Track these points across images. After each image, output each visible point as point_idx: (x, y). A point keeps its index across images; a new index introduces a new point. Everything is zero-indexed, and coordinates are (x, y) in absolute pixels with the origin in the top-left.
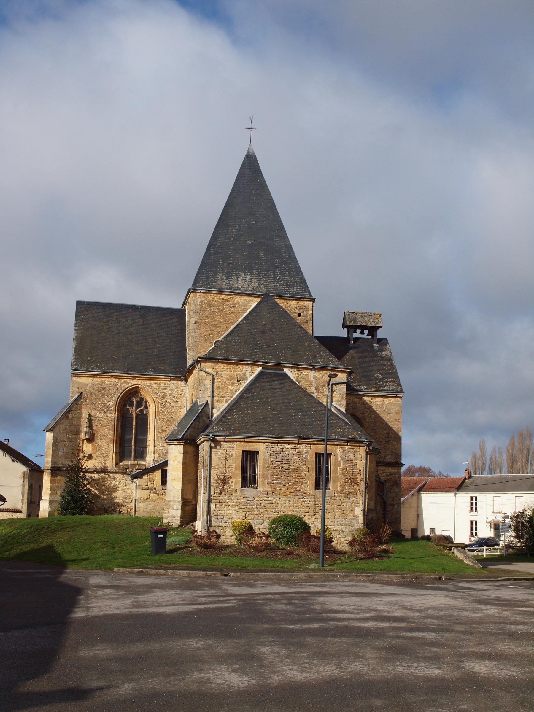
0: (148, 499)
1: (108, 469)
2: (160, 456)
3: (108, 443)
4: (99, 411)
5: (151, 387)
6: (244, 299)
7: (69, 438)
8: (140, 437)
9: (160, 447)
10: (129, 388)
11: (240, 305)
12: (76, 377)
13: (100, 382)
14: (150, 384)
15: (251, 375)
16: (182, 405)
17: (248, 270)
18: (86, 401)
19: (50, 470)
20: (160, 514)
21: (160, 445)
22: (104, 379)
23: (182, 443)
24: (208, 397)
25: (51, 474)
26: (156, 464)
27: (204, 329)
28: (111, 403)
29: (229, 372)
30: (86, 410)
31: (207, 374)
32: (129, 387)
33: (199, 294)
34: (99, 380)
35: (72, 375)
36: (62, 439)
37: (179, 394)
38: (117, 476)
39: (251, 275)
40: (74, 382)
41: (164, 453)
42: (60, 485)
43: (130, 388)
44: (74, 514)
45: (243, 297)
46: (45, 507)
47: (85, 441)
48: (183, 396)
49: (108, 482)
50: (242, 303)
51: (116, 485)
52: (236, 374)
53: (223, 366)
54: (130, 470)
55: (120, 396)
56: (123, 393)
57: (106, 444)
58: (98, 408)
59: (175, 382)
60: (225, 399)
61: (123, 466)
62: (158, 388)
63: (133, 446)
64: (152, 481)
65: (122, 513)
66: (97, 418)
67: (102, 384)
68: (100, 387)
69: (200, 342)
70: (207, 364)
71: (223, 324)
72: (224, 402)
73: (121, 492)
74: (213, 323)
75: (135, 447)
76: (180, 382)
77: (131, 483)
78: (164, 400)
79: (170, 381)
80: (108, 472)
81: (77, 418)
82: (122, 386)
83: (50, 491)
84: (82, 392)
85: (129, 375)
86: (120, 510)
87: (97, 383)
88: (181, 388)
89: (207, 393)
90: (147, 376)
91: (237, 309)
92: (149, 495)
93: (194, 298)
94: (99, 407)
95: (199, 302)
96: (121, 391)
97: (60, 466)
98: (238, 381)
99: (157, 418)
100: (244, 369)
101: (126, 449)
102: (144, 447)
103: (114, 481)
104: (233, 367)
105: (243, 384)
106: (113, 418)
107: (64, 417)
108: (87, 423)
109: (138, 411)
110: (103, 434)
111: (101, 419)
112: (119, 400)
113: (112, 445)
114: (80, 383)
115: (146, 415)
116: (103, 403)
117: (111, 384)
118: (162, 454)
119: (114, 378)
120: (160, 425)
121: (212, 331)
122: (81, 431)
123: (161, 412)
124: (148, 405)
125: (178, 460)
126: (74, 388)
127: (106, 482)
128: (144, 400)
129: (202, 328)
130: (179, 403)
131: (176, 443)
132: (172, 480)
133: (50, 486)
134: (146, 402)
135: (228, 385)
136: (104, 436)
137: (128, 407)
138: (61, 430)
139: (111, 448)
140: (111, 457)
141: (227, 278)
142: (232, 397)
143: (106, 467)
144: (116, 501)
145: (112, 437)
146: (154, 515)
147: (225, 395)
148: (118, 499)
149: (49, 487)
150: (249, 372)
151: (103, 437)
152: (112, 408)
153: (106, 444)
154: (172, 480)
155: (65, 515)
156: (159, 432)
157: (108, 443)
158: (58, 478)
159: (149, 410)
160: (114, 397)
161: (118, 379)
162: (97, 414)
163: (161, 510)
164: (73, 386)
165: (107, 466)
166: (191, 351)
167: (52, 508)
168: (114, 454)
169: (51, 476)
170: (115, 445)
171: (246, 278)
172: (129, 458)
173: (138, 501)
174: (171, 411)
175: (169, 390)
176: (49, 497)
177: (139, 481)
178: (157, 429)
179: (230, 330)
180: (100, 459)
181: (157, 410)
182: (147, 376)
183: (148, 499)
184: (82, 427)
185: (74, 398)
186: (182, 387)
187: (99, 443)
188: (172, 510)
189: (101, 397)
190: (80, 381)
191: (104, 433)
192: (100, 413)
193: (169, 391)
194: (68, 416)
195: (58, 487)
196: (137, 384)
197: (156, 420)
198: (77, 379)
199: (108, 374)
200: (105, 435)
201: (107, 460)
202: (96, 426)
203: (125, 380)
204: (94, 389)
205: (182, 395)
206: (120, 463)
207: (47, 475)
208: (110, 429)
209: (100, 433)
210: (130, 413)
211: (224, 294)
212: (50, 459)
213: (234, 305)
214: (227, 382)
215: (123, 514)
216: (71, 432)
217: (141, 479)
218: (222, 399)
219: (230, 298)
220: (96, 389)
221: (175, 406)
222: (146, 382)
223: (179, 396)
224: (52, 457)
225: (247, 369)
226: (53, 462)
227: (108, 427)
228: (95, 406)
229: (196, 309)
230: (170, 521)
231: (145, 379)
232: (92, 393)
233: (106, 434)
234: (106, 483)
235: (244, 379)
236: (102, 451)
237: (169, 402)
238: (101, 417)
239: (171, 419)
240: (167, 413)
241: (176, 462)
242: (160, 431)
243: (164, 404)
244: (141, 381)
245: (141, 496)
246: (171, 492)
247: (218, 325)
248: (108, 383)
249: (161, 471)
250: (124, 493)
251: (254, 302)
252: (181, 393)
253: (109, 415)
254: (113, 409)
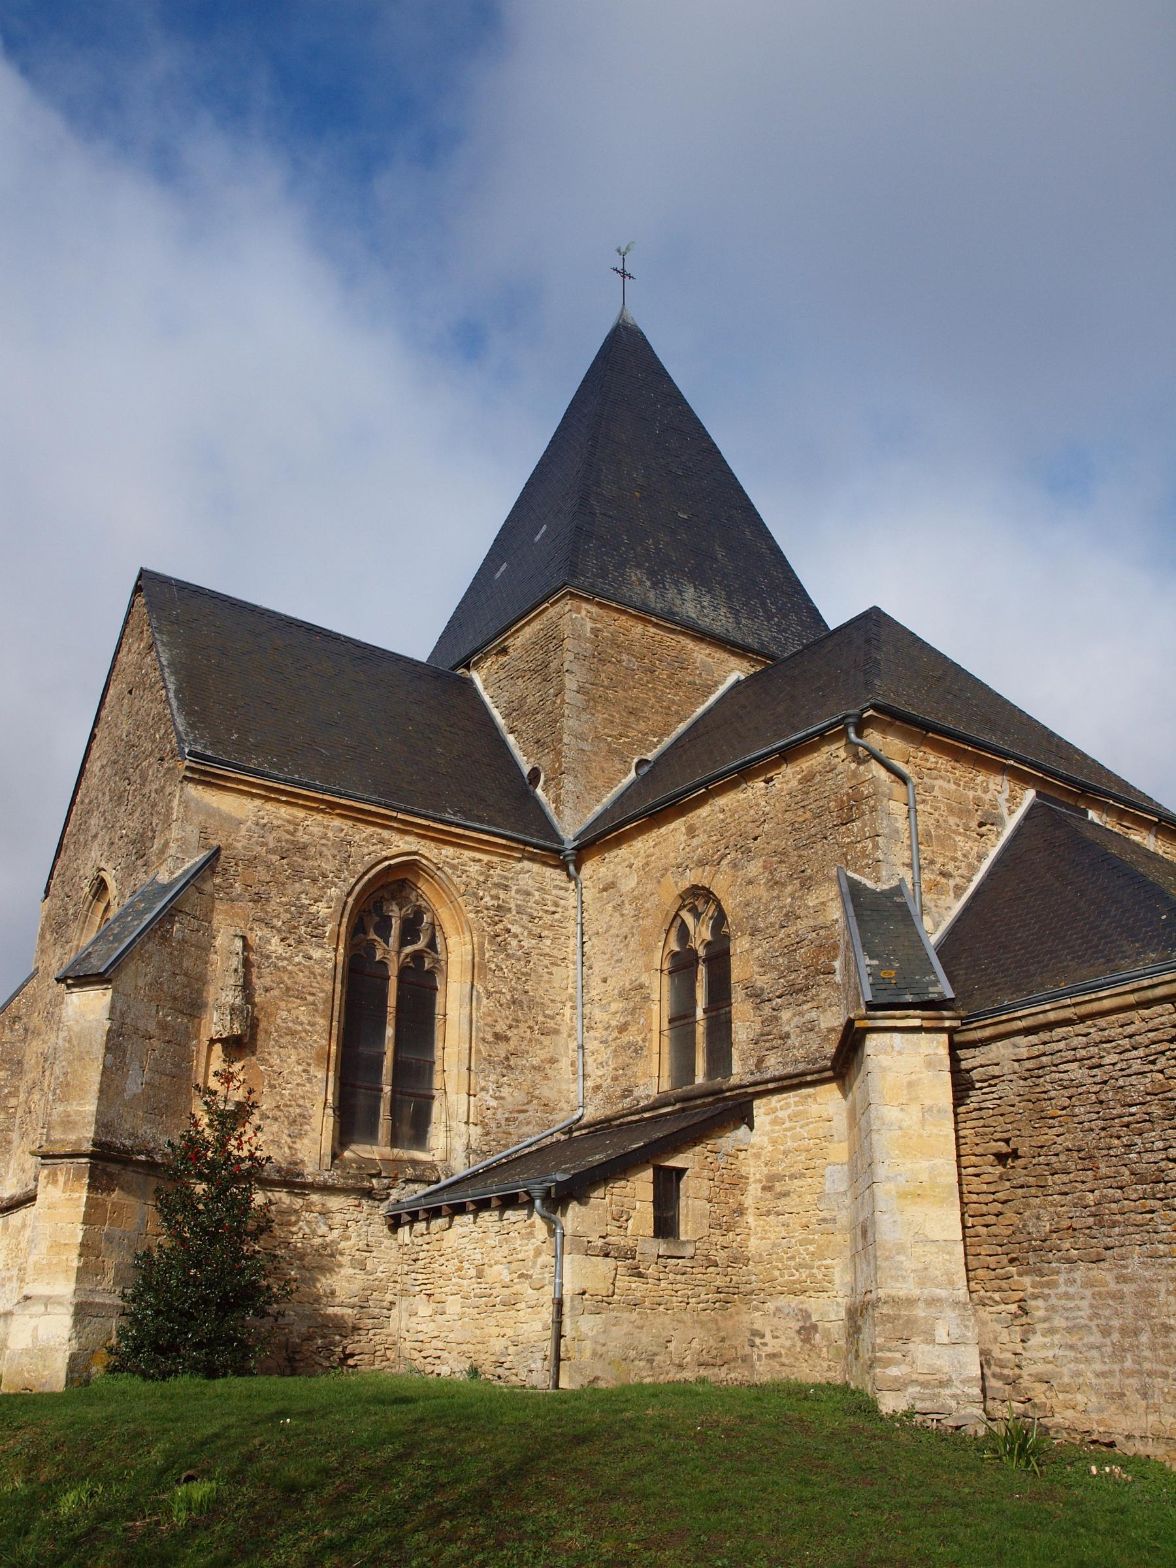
0: (603, 1303)
1: (306, 1172)
2: (488, 1134)
3: (309, 1065)
4: (279, 931)
5: (459, 873)
6: (707, 651)
7: (163, 1026)
8: (409, 1056)
9: (488, 1098)
10: (387, 863)
11: (697, 668)
12: (200, 788)
13: (288, 821)
14: (456, 861)
15: (1011, 812)
16: (555, 953)
17: (702, 579)
18: (232, 886)
19: (90, 1155)
20: (652, 1368)
21: (488, 1092)
22: (301, 814)
23: (947, 1024)
24: (904, 864)
25: (90, 1177)
26: (479, 1165)
27: (605, 716)
28: (322, 909)
29: (953, 787)
30: (229, 921)
31: (893, 777)
32: (386, 859)
33: (589, 607)
34: (285, 812)
35: (189, 774)
36: (141, 1025)
37: (546, 912)
38: (335, 1202)
39: (709, 596)
40: (192, 805)
41: (503, 1123)
42: (118, 1232)
43: (392, 862)
44: (212, 1373)
45: (703, 646)
46: (41, 1333)
47: (218, 1047)
48: (559, 921)
49: (300, 1228)
50: (703, 663)
51: (332, 1241)
52: (974, 798)
53: (934, 760)
54: (386, 1181)
55: (358, 888)
56: (366, 878)
57: (301, 1068)
58: (275, 921)
59: (535, 867)
60: (952, 883)
61: (363, 1163)
62: (482, 879)
63: (387, 1089)
64: (622, 1218)
65: (351, 1362)
66: (268, 957)
67: (296, 830)
68: (287, 841)
69: (595, 754)
70: (889, 738)
71: (657, 712)
72: (952, 894)
73: (351, 1271)
74: (629, 703)
75: (393, 1091)
76: (549, 872)
77: (385, 1237)
78: (500, 926)
79: (520, 860)
80: (304, 1186)
81: (198, 947)
82: (366, 851)
83: (80, 1255)
84: (219, 850)
85: (395, 814)
86: (343, 1351)
87: (276, 823)
88: (554, 892)
89: (898, 849)
90: (453, 829)
91: (691, 678)
92: (613, 1284)
93: (574, 616)
94: (278, 916)
95: (589, 629)
96: (360, 869)
97: (128, 1143)
98: (981, 825)
99: (479, 987)
100: (992, 786)
101: (361, 1100)
102: (420, 1096)
103: (325, 1224)
104: (962, 771)
105: (992, 837)
106: (330, 965)
107: (154, 931)
108: (236, 970)
109: (407, 956)
110: (290, 1025)
111: (285, 963)
112: (351, 900)
113: (321, 1074)
114: (211, 812)
115: (431, 974)
116: (295, 905)
117: (325, 836)
118: (494, 1125)
119: (338, 815)
120: (489, 1015)
121: (626, 725)
122: (205, 1005)
123: (493, 966)
124: (438, 940)
125: (928, 1102)
126: (189, 828)
127: (294, 1229)
128: (426, 918)
129: (598, 711)
130: (548, 942)
131: (917, 1023)
132: (903, 1195)
133: (81, 1233)
134: (433, 925)
135: (955, 832)
136: (293, 1033)
137: (373, 936)
138: (141, 983)
139: (318, 1088)
140: (316, 1121)
141: (654, 585)
142: (970, 880)
143: (296, 1164)
144: (330, 1311)
145: (324, 1042)
146: (632, 1374)
147: (950, 867)
148: (338, 1300)
149: (76, 1235)
150: (1007, 800)
151: (289, 1038)
152: (328, 929)
153: (301, 1068)
154: (903, 1195)
155: (165, 1375)
156: (484, 1039)
157: (309, 1065)
158: (115, 1195)
159: (442, 957)
160: (335, 885)
161: (350, 823)
162: (269, 942)
163: (659, 1350)
164: (185, 819)
165: (302, 1161)
166: (571, 778)
167: (83, 1340)
168: (330, 1111)
169: (91, 1187)
170: (331, 1074)
171: (700, 597)
172: (370, 1136)
173: (572, 1308)
174: (524, 970)
175: (517, 892)
176: (73, 1286)
177: (574, 1217)
178: (478, 1029)
179: (674, 735)
180: (275, 1128)
181: (477, 959)
182: (453, 829)
183: (603, 1303)
184: (212, 989)
185: (187, 865)
186: (556, 887)
187: (275, 1061)
188: (926, 1348)
189: (288, 878)
190: (215, 805)
191: (293, 1021)
192: (282, 940)
193: (517, 896)
194: (167, 931)
195: (109, 1238)
196: (415, 853)
197: (475, 993)
198: (204, 794)
199: (320, 796)
200: (296, 1032)
201: (300, 1136)
202: (267, 991)
203: (374, 829)
204: (263, 844)
205: (557, 916)
206: (343, 1152)
207: (61, 1179)
208: (316, 1010)
209: (279, 1021)
210: (378, 958)
211: (656, 625)
212: (89, 1107)
213: (681, 662)
214: (952, 820)
215: (356, 1365)
216: (175, 999)
217: (583, 1208)
218: (944, 880)
219: (671, 640)
220: (271, 845)
221: (534, 952)
222: (444, 852)
223: (548, 918)
224: (99, 1098)
225: (999, 788)
226: (103, 1124)
227: (310, 998)
228: (267, 913)
229: (580, 650)
230: (919, 1406)
231: (443, 839)
232: (255, 858)
233: (300, 1028)
234: (293, 1233)
235: (989, 821)
236: (282, 1095)
237: (516, 936)
238: (285, 959)
239: (524, 998)
240: (511, 976)
241: (915, 1110)
242: (490, 1038)
243: (499, 939)
244: (428, 843)
245: (585, 1285)
246: (902, 1258)
247: (642, 711)
248: (315, 830)
249: (648, 1174)
250: (361, 1276)
251: (735, 671)
252: (553, 909)
253: (317, 954)
254: (332, 931)
